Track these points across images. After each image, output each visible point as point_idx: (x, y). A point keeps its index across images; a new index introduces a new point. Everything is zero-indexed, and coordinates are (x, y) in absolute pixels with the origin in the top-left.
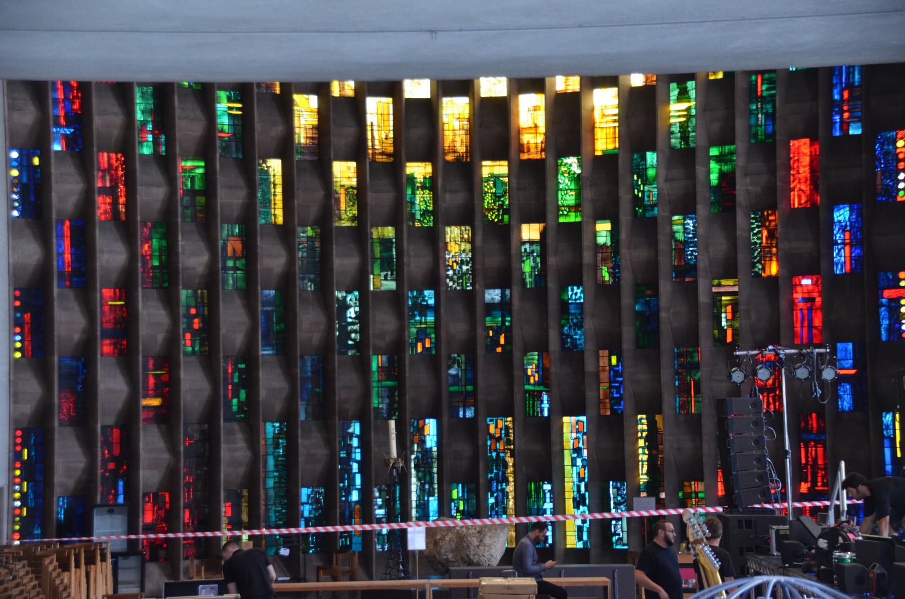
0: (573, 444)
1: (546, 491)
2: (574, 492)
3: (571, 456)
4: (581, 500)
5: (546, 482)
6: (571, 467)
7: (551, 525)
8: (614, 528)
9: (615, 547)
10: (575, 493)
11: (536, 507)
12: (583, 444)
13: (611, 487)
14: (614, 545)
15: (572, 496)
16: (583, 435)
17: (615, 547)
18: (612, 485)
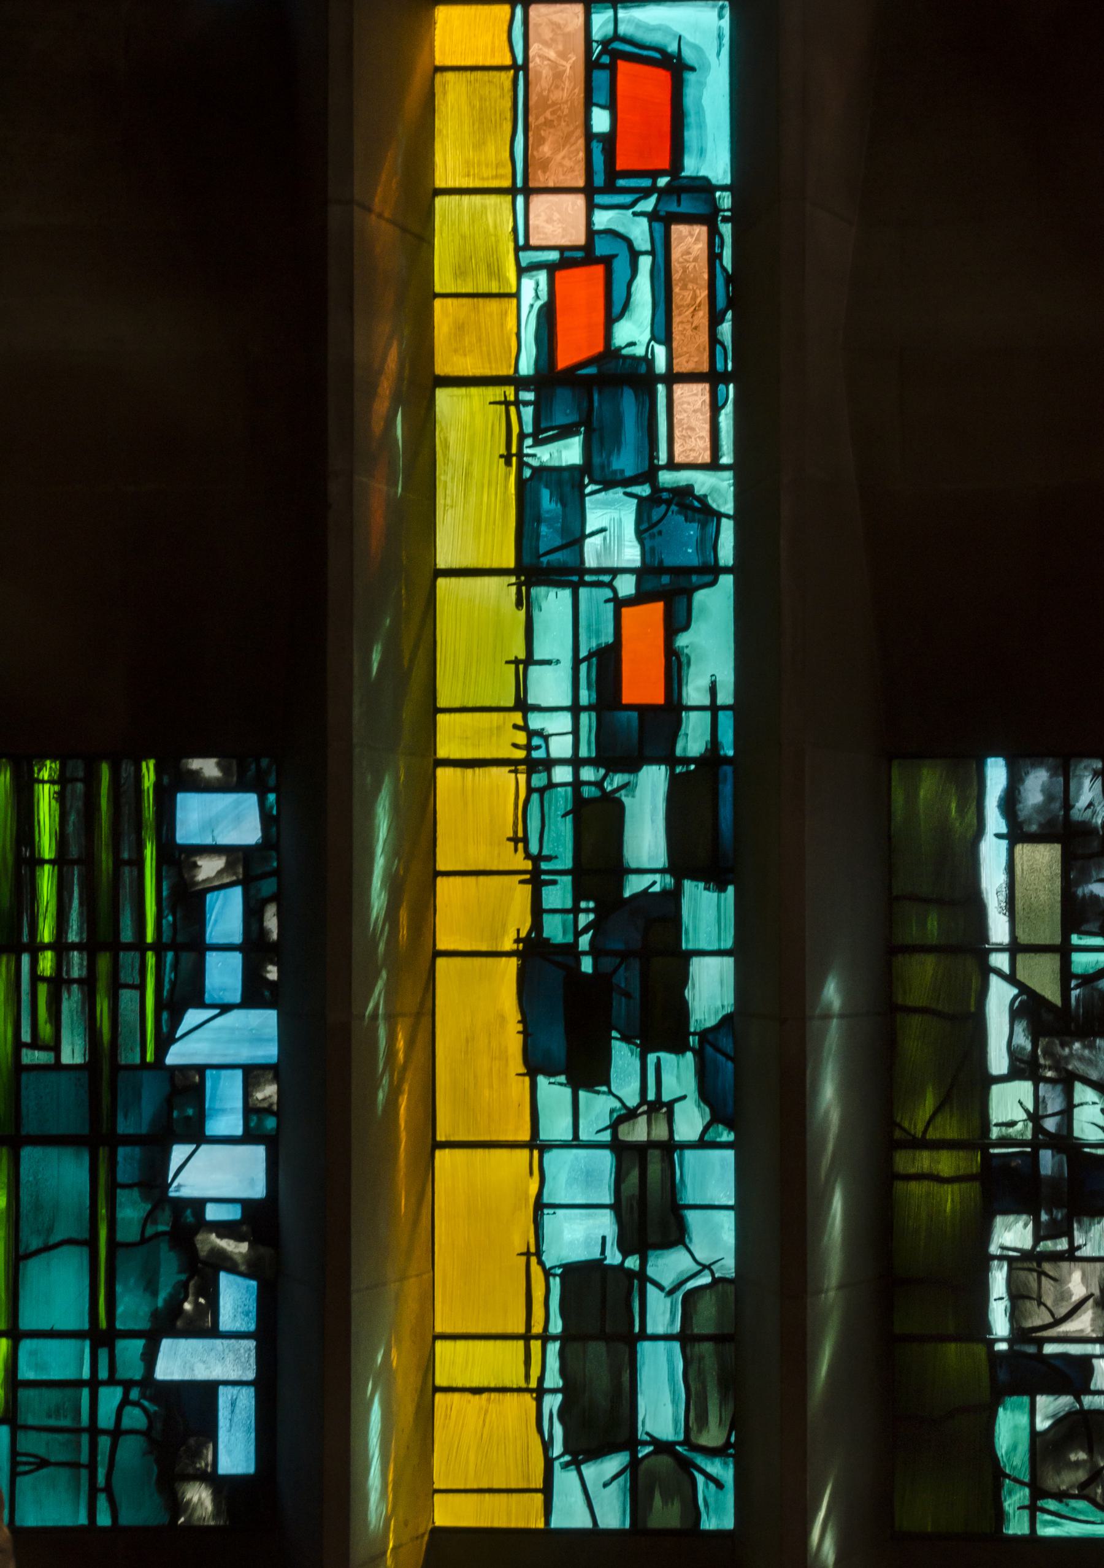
0: (548, 316)
1: (209, 868)
2: (536, 880)
3: (512, 456)
4: (628, 978)
5: (209, 767)
6: (502, 590)
7: (252, 1269)
8: (1017, 1296)
9: (1017, 1526)
10: (558, 895)
11: (72, 1052)
12: (663, 332)
13: (995, 821)
14: (1015, 1500)
15: (519, 920)
16: (663, 221)
17: (1017, 1526)
18: (1010, 803)
